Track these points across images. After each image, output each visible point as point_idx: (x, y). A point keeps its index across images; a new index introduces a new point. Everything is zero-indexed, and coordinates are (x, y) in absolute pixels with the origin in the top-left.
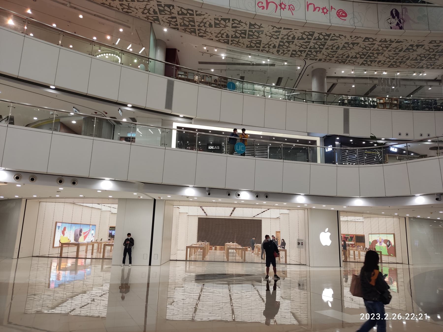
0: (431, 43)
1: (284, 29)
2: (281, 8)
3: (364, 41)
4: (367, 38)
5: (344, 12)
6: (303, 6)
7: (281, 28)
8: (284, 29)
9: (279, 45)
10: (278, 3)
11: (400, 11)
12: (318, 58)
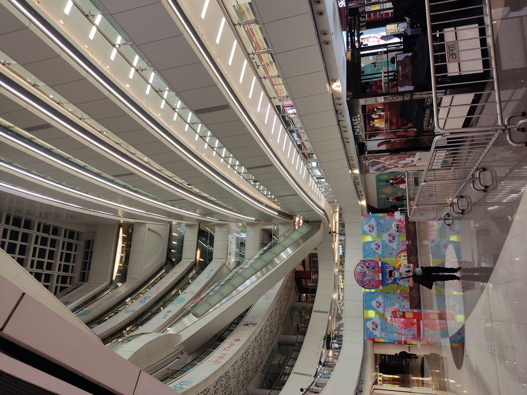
0: (267, 321)
1: (235, 363)
2: (223, 357)
3: (256, 342)
4: (255, 338)
5: (237, 339)
6: (226, 351)
7: (234, 365)
8: (235, 363)
9: (238, 383)
10: (219, 358)
11: (246, 323)
12: (250, 378)
